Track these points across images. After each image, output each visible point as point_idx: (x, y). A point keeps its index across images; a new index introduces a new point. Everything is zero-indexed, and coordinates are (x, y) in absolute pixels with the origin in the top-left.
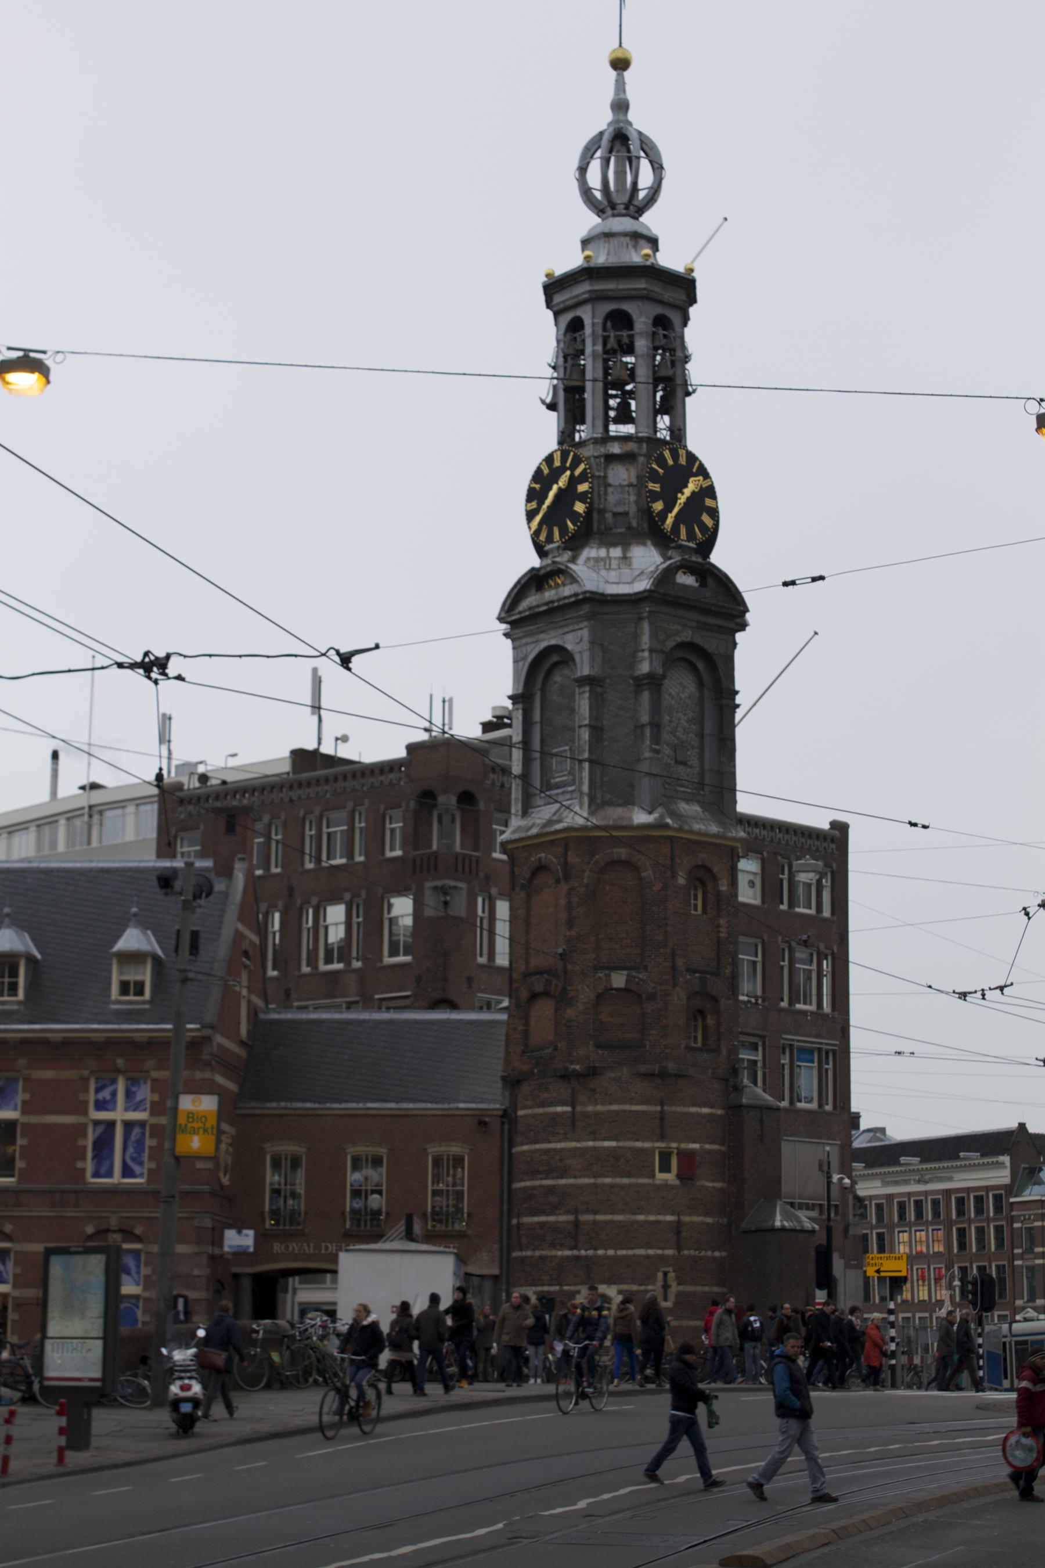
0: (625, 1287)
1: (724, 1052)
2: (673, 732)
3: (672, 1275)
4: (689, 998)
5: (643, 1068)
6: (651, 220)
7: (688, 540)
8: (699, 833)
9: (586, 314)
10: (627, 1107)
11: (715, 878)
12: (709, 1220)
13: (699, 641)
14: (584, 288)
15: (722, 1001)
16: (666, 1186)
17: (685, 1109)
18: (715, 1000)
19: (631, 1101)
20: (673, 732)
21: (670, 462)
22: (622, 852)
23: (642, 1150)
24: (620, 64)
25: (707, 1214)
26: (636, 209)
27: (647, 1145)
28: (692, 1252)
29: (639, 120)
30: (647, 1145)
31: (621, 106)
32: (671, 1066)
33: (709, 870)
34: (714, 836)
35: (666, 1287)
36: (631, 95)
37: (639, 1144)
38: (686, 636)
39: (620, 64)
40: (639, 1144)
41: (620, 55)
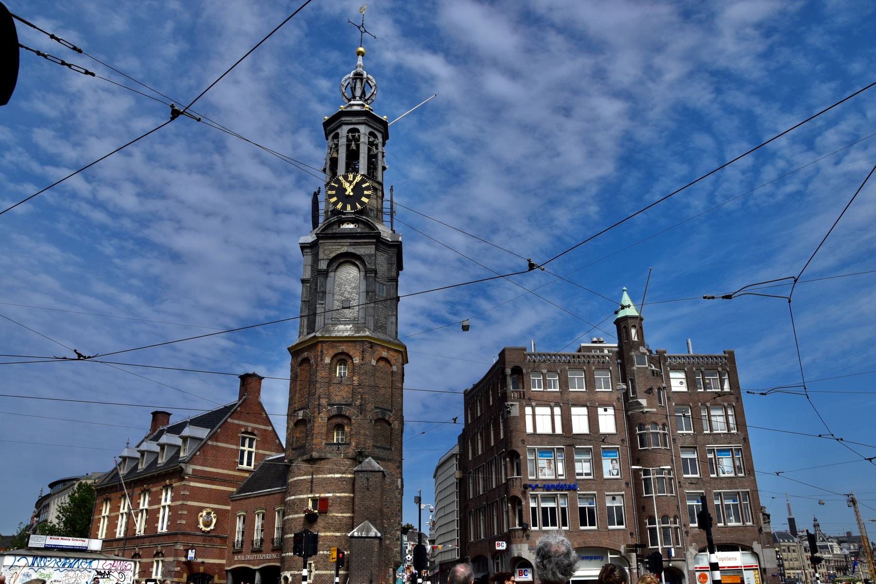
0: (293, 572)
1: (353, 444)
2: (342, 295)
3: (313, 565)
4: (329, 419)
5: (305, 457)
8: (336, 337)
10: (299, 478)
11: (351, 358)
12: (338, 534)
13: (351, 250)
17: (325, 476)
18: (349, 419)
19: (301, 475)
20: (342, 295)
23: (303, 499)
25: (337, 531)
27: (305, 496)
28: (325, 552)
30: (305, 496)
32: (315, 454)
33: (347, 355)
34: (346, 337)
35: (310, 572)
37: (302, 496)
38: (344, 249)
40: (302, 496)
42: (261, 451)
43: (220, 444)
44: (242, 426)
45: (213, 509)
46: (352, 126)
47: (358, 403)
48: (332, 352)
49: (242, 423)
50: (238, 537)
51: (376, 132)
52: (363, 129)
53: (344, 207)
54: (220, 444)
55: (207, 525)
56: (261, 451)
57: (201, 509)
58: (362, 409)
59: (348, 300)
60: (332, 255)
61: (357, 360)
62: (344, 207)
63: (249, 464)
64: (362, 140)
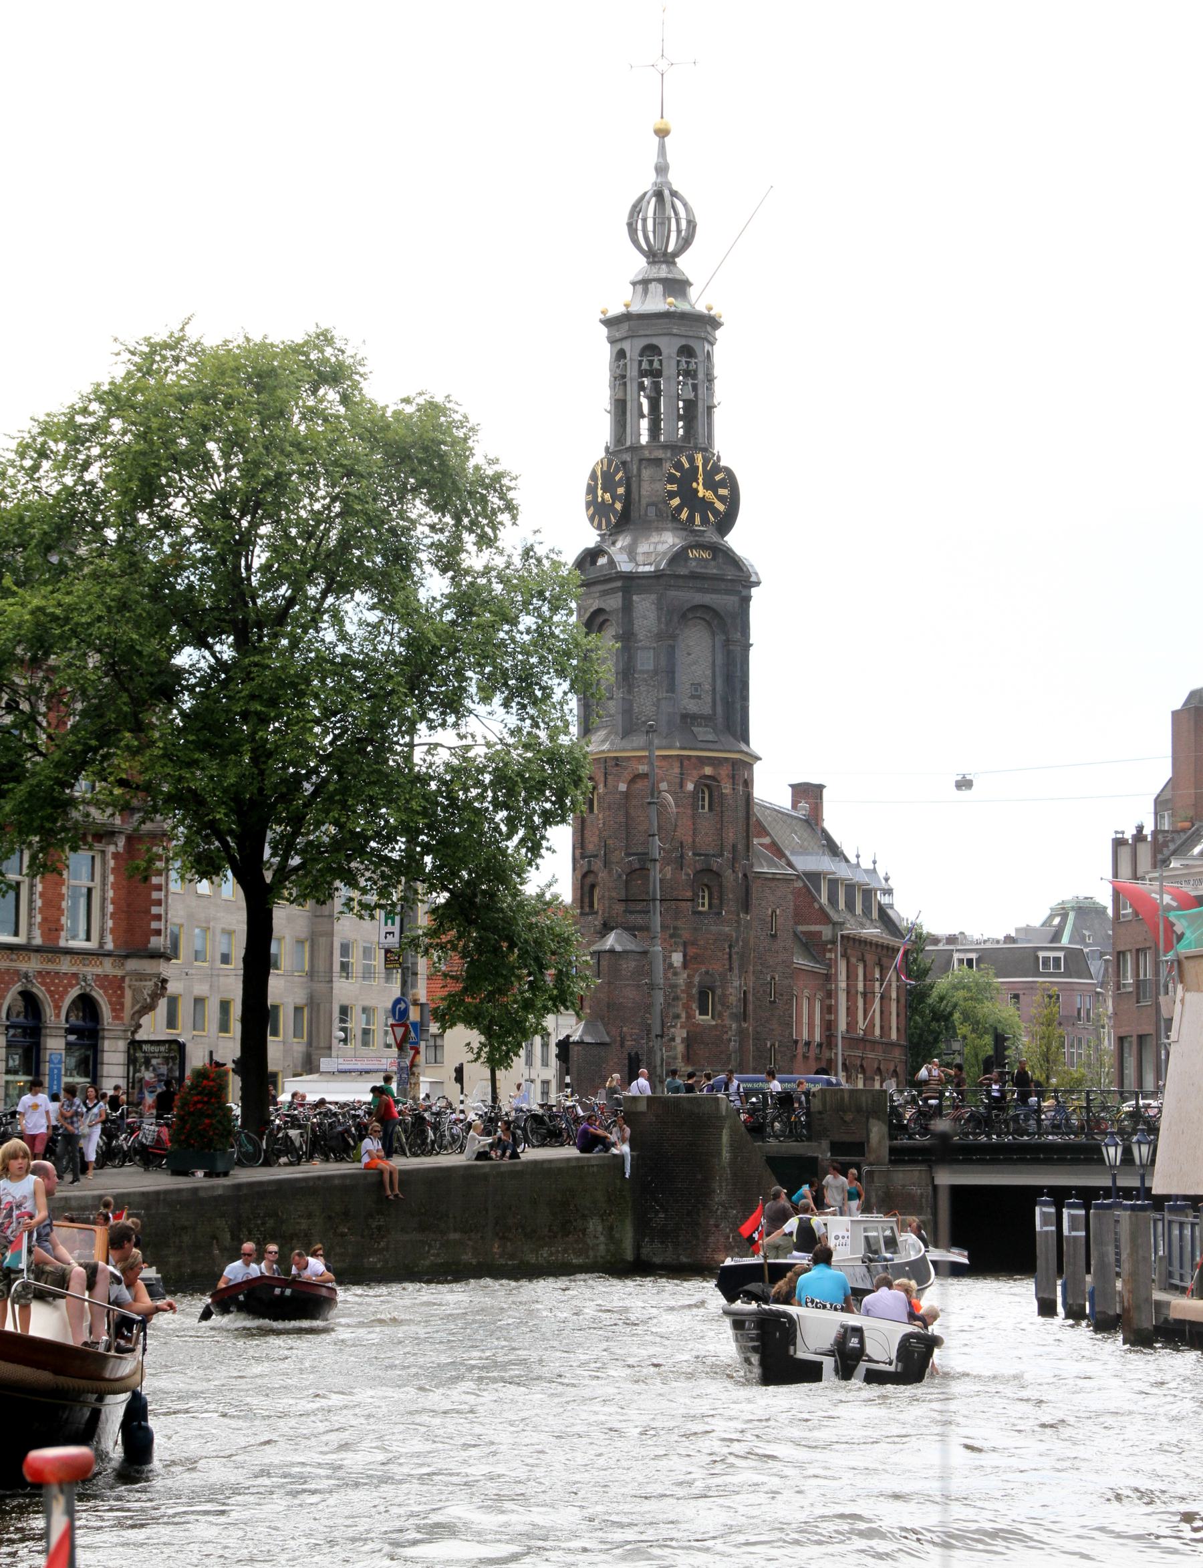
6: (686, 264)
7: (702, 525)
9: (626, 346)
14: (625, 327)
21: (687, 466)
22: (642, 769)
24: (662, 133)
26: (669, 259)
29: (676, 179)
31: (662, 169)
36: (670, 158)
39: (662, 133)
41: (662, 126)
46: (683, 342)
48: (695, 774)
62: (691, 518)
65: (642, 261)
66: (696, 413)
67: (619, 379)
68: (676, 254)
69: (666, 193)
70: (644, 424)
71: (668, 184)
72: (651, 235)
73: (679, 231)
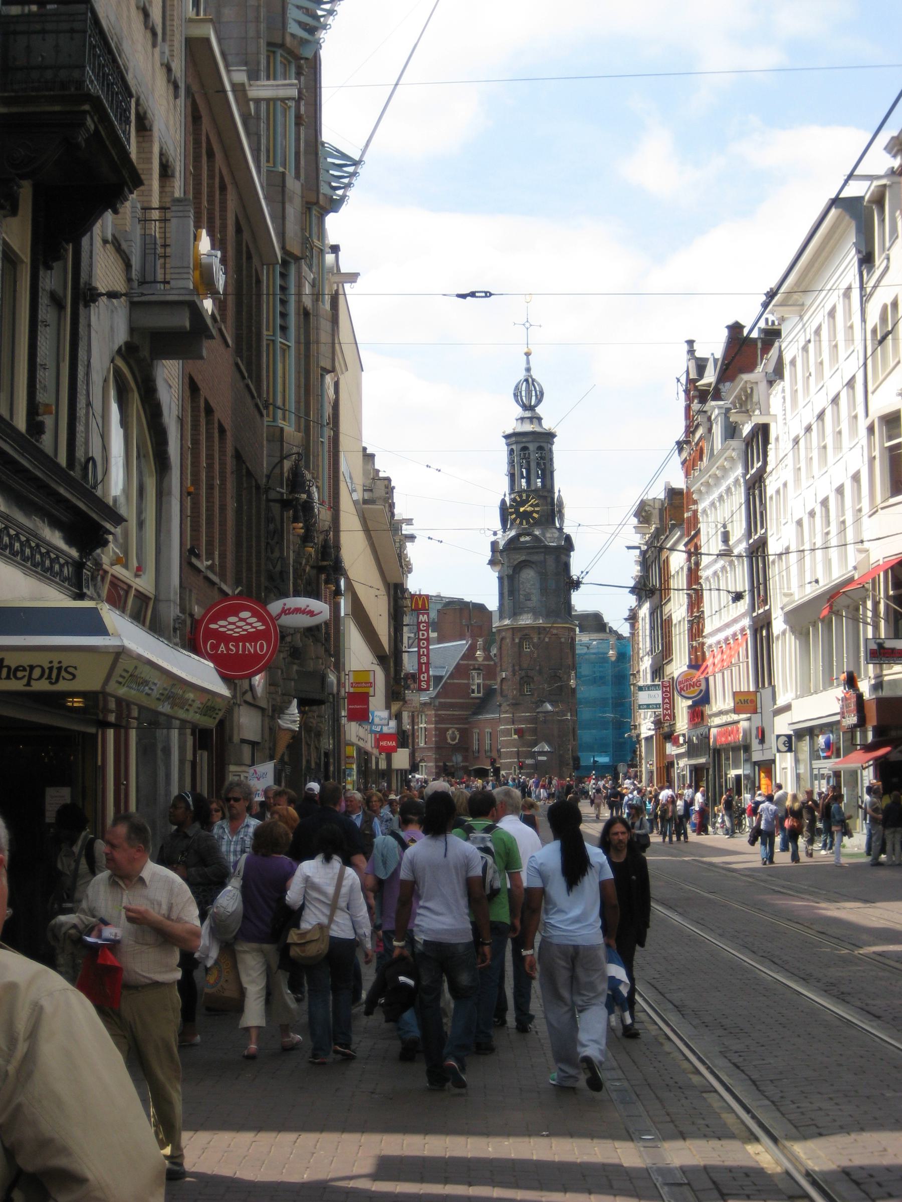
11: (532, 638)
14: (513, 439)
15: (535, 679)
16: (515, 739)
24: (528, 354)
31: (528, 370)
36: (532, 365)
38: (523, 558)
39: (528, 354)
42: (487, 682)
43: (456, 681)
44: (471, 665)
45: (456, 728)
46: (523, 445)
47: (537, 668)
48: (519, 635)
49: (470, 662)
50: (476, 747)
51: (542, 444)
52: (532, 447)
53: (521, 523)
54: (456, 681)
55: (453, 739)
56: (487, 682)
57: (447, 729)
58: (540, 672)
59: (529, 594)
60: (516, 563)
61: (535, 640)
63: (479, 692)
64: (532, 457)
65: (519, 411)
66: (547, 473)
67: (511, 463)
68: (536, 406)
69: (530, 380)
70: (524, 481)
71: (531, 377)
72: (524, 398)
73: (536, 395)
